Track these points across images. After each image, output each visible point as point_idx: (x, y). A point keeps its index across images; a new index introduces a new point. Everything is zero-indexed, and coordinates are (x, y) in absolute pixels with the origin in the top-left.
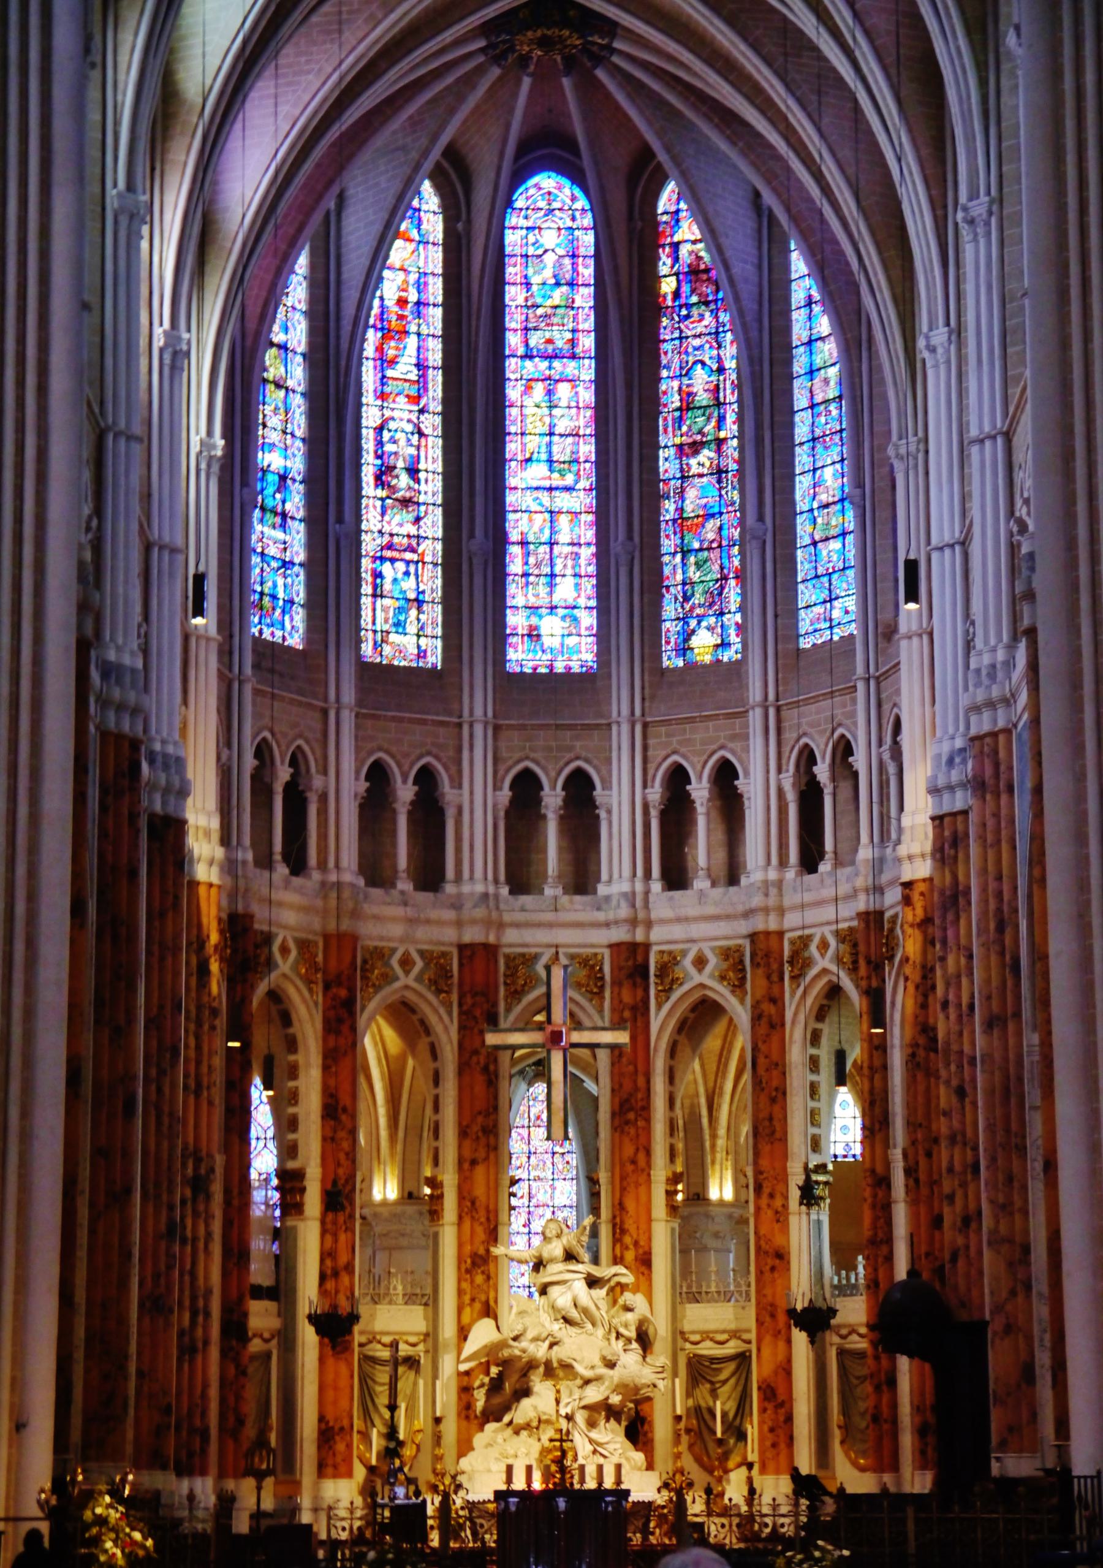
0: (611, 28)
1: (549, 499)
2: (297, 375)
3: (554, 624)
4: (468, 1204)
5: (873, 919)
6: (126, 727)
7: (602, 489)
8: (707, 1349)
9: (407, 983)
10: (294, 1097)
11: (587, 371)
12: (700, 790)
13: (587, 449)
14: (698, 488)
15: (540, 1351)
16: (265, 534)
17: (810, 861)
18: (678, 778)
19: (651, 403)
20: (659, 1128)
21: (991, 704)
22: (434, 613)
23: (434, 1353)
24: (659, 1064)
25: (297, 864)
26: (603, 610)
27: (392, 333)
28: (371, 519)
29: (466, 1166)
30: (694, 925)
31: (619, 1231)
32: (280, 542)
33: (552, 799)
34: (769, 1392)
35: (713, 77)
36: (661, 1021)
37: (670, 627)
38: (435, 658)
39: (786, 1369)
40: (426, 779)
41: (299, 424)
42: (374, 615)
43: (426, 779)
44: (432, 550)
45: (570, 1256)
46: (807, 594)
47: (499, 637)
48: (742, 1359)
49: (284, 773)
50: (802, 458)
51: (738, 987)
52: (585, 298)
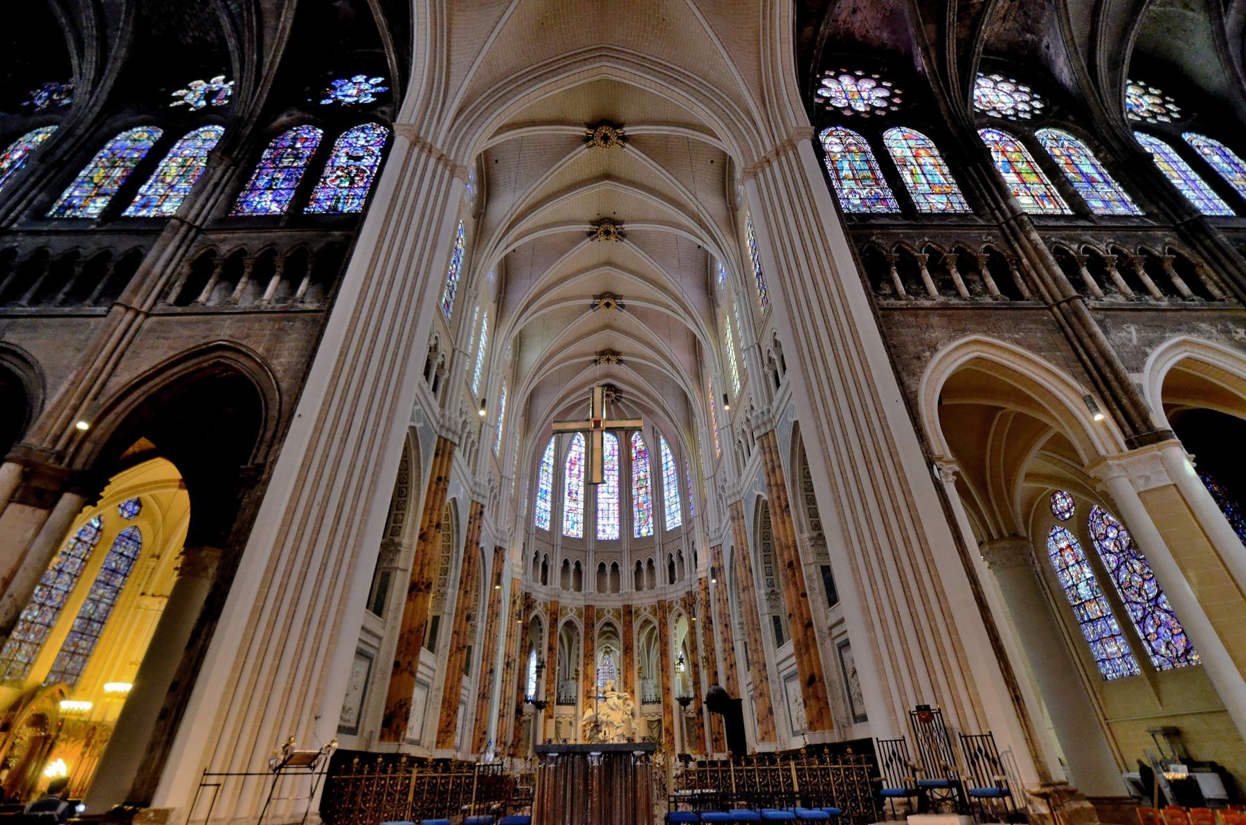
0: (621, 391)
1: (608, 498)
2: (551, 470)
3: (609, 529)
4: (586, 676)
5: (689, 594)
6: (480, 500)
7: (620, 498)
8: (650, 718)
9: (571, 615)
10: (541, 645)
11: (616, 473)
12: (644, 566)
13: (617, 490)
14: (641, 496)
15: (604, 718)
16: (540, 503)
17: (672, 582)
18: (639, 563)
19: (630, 480)
20: (636, 654)
21: (734, 494)
22: (581, 526)
23: (576, 720)
24: (635, 637)
25: (545, 583)
26: (620, 525)
27: (573, 463)
28: (567, 503)
29: (586, 665)
30: (643, 600)
31: (626, 683)
32: (544, 506)
33: (608, 569)
34: (667, 731)
35: (644, 398)
36: (636, 625)
37: (636, 529)
38: (581, 536)
39: (672, 723)
40: (578, 564)
41: (551, 481)
42: (566, 525)
43: (578, 564)
44: (581, 511)
45: (613, 690)
46: (668, 518)
47: (596, 532)
48: (659, 721)
49: (542, 559)
50: (666, 488)
51: (655, 615)
52: (616, 458)
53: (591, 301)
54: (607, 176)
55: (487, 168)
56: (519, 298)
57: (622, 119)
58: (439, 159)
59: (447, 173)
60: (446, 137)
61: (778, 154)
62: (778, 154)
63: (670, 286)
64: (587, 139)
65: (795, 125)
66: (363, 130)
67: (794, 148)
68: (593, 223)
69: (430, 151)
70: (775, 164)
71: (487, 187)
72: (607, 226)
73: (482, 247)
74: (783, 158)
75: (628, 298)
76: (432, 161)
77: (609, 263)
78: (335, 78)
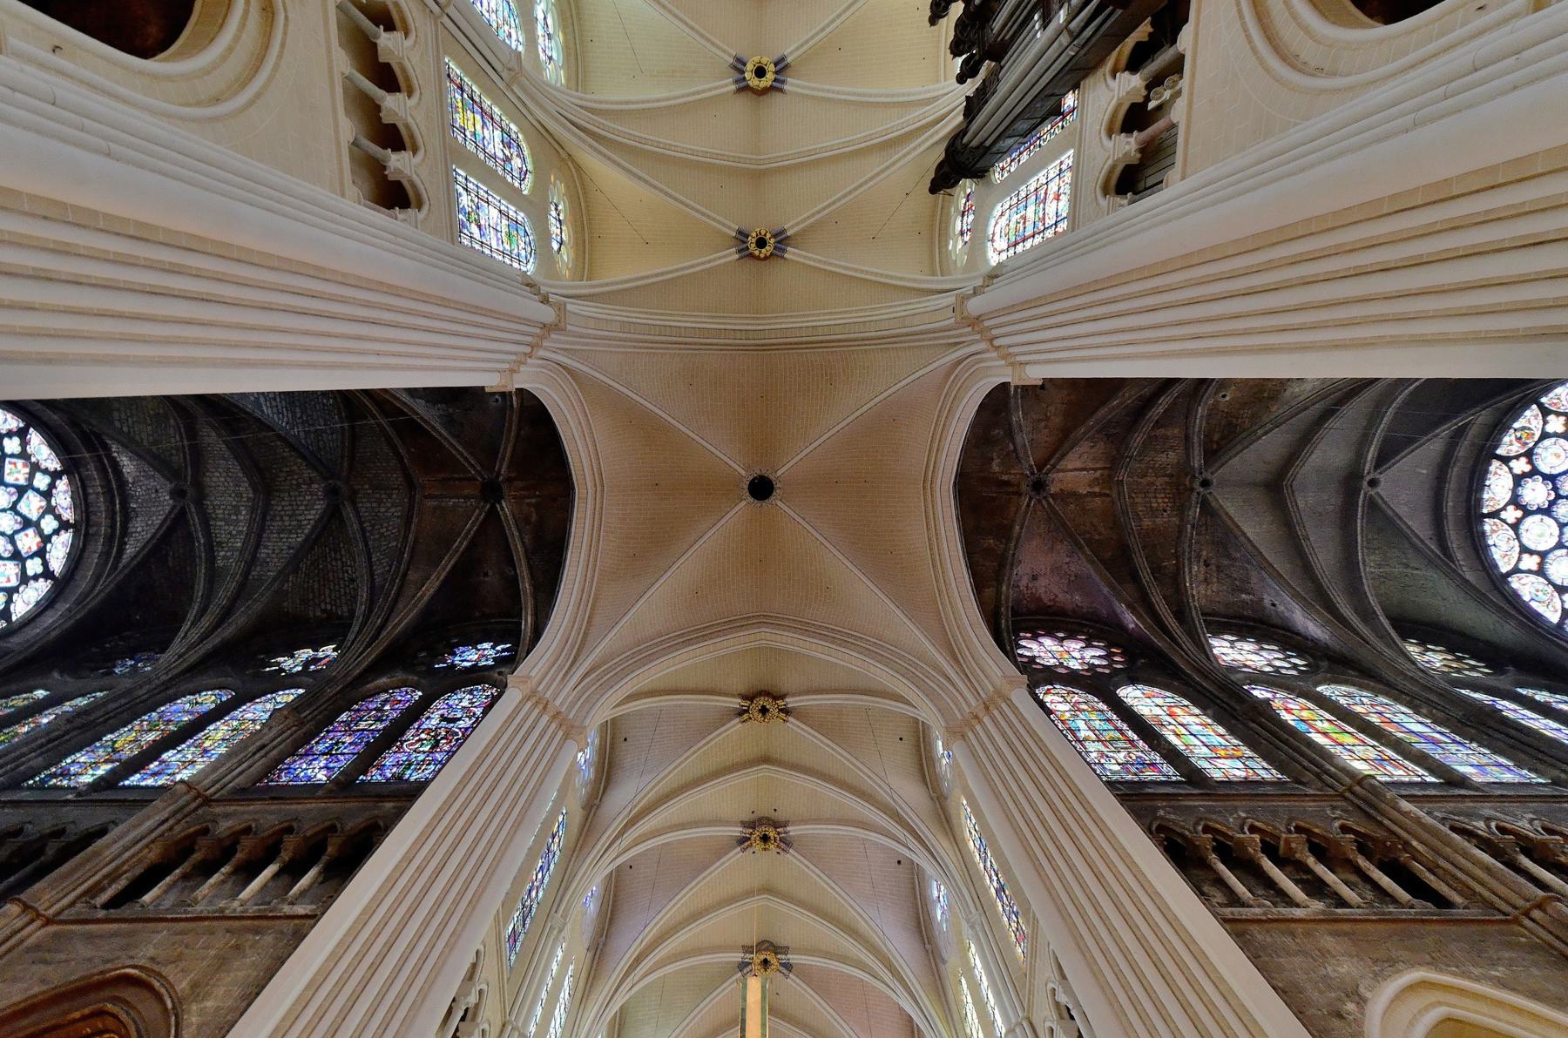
53: (737, 957)
54: (766, 760)
55: (612, 748)
56: (627, 945)
57: (784, 690)
58: (554, 717)
59: (561, 733)
60: (568, 695)
61: (987, 708)
62: (987, 708)
63: (863, 926)
64: (741, 713)
65: (999, 673)
66: (471, 692)
67: (1008, 700)
68: (745, 824)
69: (545, 708)
70: (986, 720)
71: (607, 770)
72: (765, 831)
73: (585, 850)
74: (996, 713)
75: (800, 951)
76: (545, 718)
77: (767, 890)
78: (457, 646)
